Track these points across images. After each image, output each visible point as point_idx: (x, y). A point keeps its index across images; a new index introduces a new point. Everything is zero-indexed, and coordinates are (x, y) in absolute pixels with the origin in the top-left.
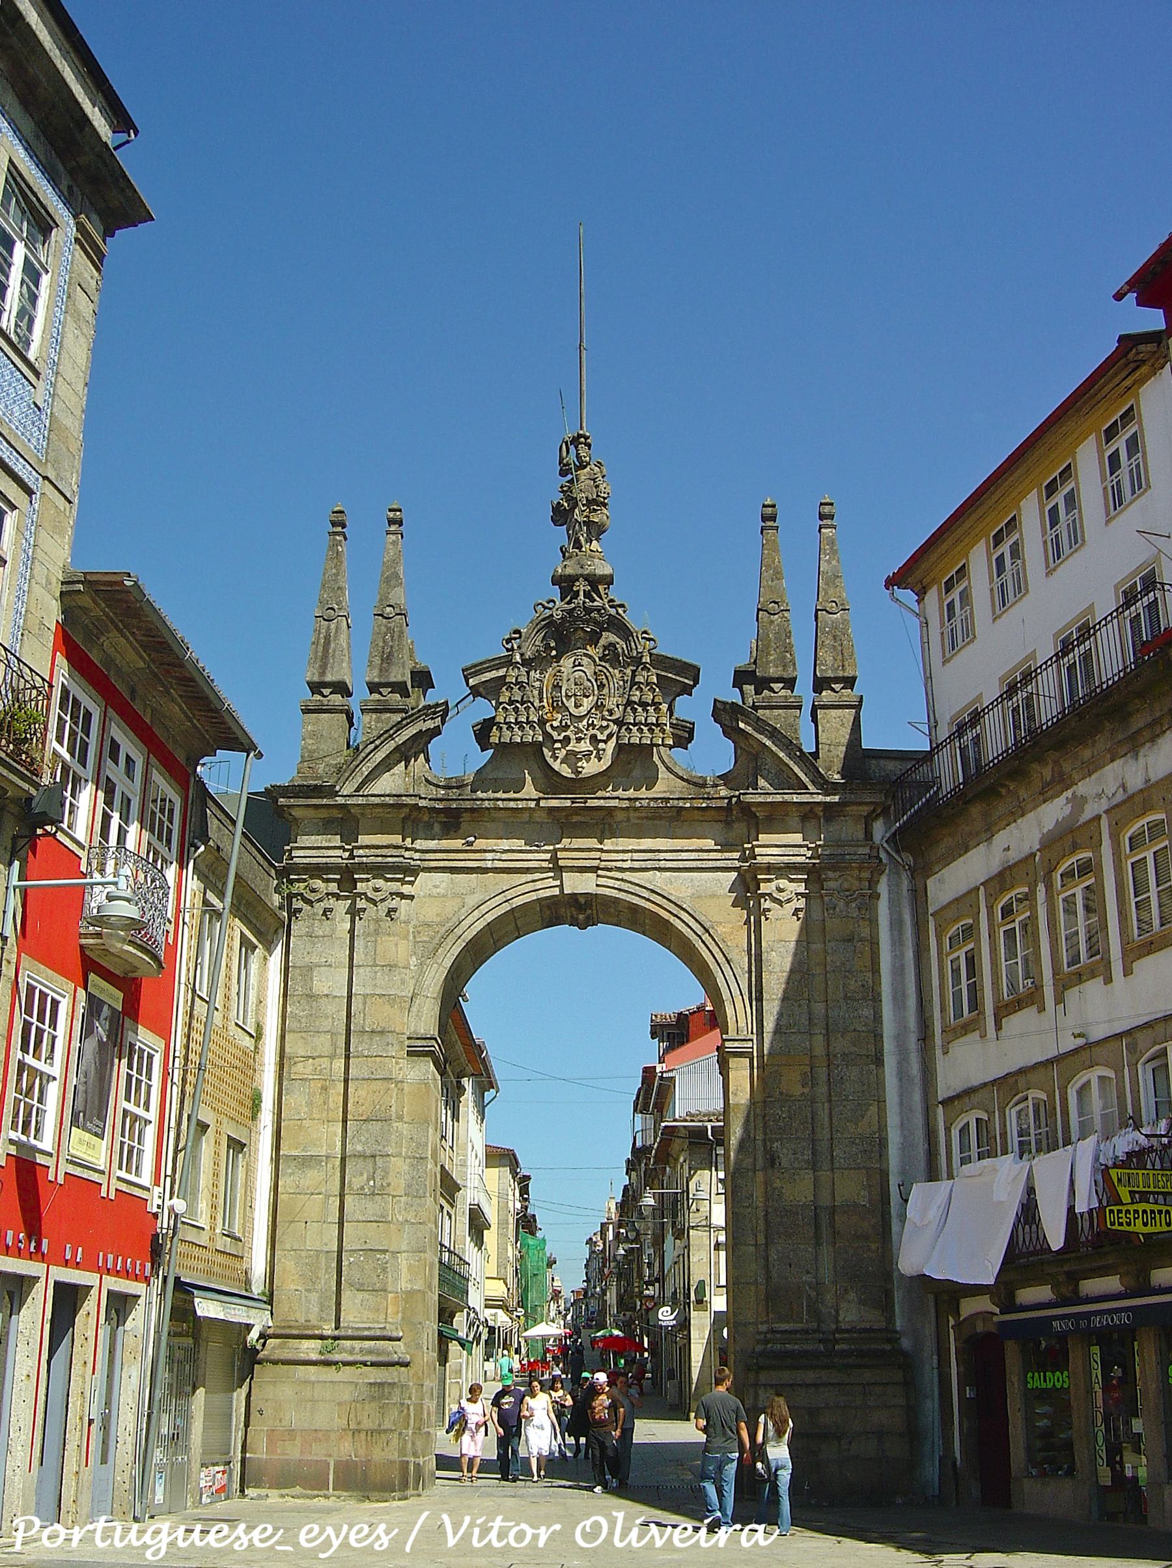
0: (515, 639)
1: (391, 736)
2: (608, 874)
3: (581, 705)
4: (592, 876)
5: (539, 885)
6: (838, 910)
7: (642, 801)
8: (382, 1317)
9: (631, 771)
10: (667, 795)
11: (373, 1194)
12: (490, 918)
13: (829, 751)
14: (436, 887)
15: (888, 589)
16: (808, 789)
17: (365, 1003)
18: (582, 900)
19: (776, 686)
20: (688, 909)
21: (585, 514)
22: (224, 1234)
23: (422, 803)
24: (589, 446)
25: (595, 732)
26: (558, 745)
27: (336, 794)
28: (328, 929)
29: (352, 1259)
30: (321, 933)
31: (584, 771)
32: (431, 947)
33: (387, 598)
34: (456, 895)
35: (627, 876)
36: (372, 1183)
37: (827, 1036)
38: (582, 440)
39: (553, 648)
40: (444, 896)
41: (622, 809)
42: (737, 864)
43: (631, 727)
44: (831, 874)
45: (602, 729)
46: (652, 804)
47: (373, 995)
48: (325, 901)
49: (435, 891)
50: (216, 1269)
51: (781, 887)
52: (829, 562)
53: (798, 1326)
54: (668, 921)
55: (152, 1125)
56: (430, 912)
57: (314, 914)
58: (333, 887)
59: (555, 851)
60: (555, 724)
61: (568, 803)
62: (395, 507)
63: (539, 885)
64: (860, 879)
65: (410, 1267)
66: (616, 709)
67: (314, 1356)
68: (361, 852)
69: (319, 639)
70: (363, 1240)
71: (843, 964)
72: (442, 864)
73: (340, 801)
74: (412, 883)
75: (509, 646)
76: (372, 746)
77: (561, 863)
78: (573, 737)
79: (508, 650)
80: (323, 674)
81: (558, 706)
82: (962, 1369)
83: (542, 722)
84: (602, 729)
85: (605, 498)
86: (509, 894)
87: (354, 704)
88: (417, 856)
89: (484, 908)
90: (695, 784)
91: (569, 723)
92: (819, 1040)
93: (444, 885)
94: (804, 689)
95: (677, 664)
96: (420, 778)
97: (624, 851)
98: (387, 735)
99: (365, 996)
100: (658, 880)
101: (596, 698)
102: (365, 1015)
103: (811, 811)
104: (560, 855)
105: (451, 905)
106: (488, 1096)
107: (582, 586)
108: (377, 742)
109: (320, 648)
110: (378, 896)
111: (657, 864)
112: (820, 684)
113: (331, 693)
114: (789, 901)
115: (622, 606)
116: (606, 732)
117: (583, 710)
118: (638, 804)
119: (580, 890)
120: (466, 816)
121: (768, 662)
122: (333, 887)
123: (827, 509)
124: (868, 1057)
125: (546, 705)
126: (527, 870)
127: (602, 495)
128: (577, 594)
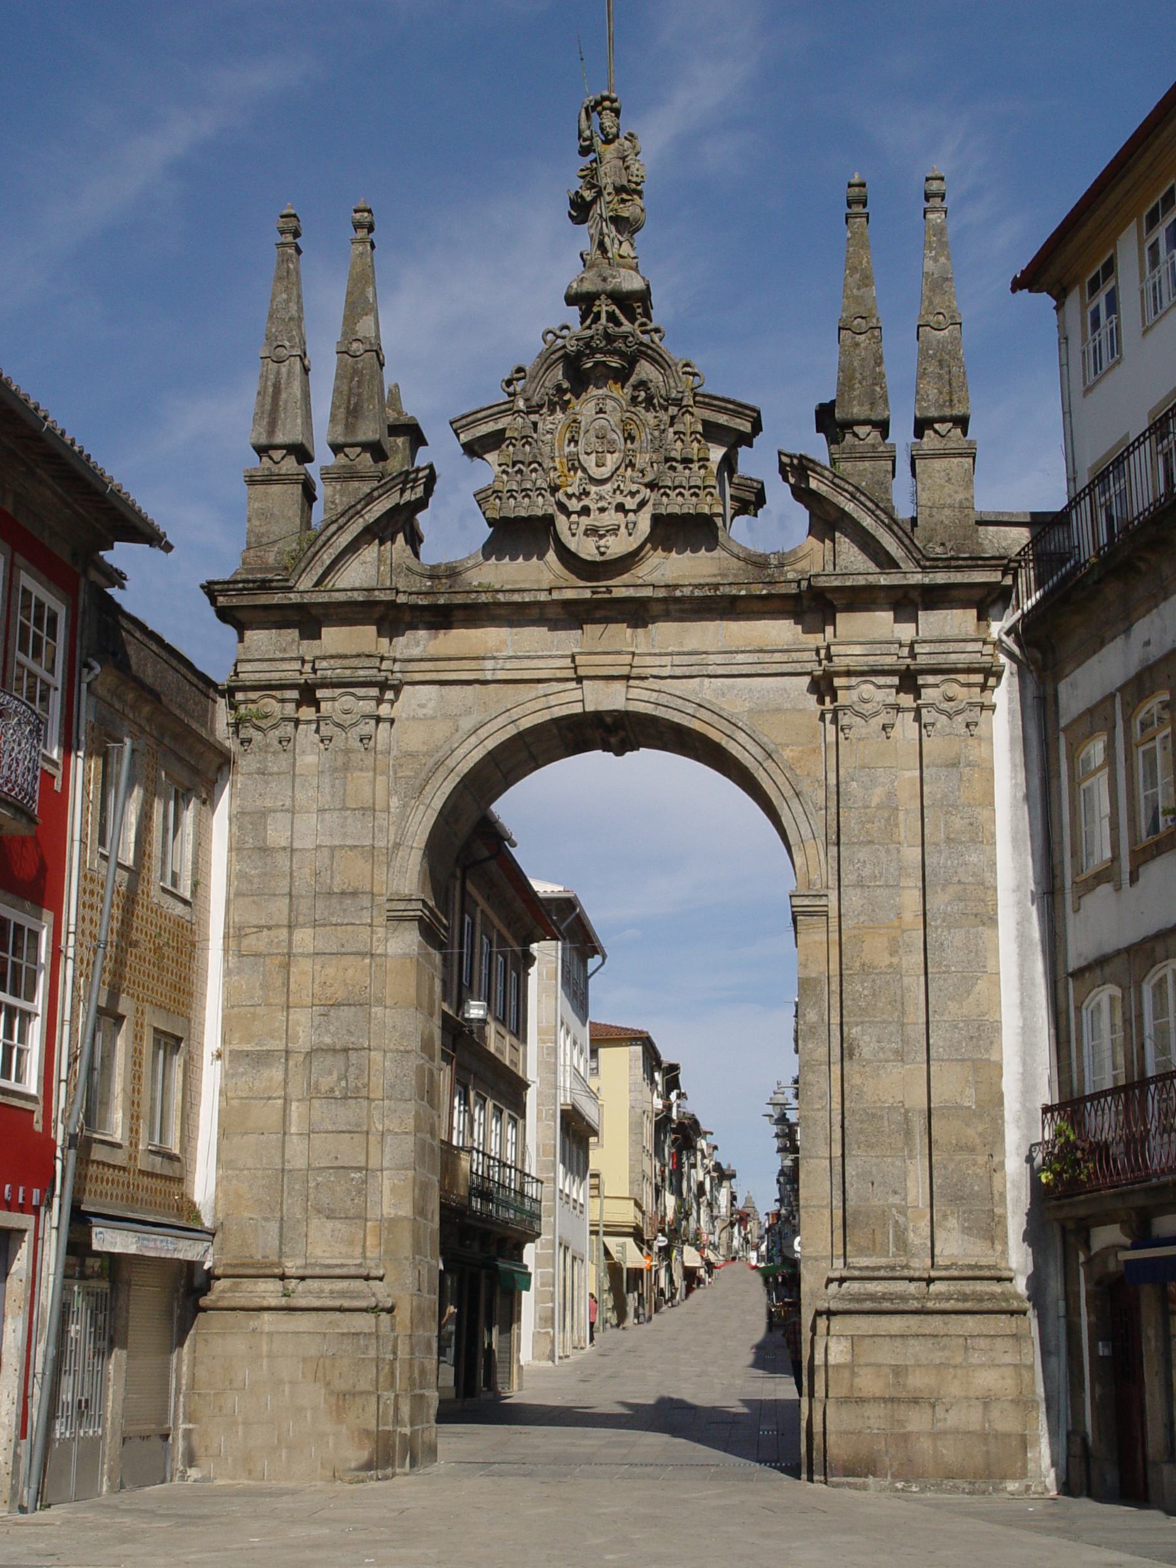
0: (518, 379)
1: (358, 513)
3: (603, 465)
4: (619, 686)
5: (553, 700)
7: (685, 589)
8: (358, 1250)
10: (718, 580)
11: (345, 1098)
12: (491, 744)
13: (931, 516)
14: (421, 706)
16: (900, 567)
18: (608, 720)
19: (862, 430)
20: (744, 728)
21: (611, 206)
22: (151, 1151)
23: (402, 599)
24: (617, 112)
25: (619, 498)
27: (290, 589)
28: (284, 764)
29: (320, 1179)
30: (275, 769)
31: (609, 552)
32: (418, 782)
33: (354, 332)
34: (446, 717)
36: (343, 1083)
38: (607, 104)
39: (565, 391)
40: (433, 718)
41: (658, 600)
43: (668, 491)
44: (930, 679)
45: (633, 494)
46: (697, 593)
47: (342, 847)
48: (280, 729)
49: (421, 712)
50: (141, 1194)
52: (935, 260)
53: (882, 1261)
55: (38, 1019)
57: (268, 745)
59: (573, 657)
60: (570, 490)
62: (362, 206)
63: (553, 700)
65: (393, 1190)
66: (649, 469)
67: (273, 1302)
68: (324, 664)
69: (265, 387)
70: (332, 1155)
71: (945, 796)
73: (294, 598)
75: (511, 389)
76: (334, 527)
77: (582, 672)
78: (593, 506)
79: (510, 395)
80: (271, 432)
81: (575, 465)
82: (1093, 1319)
84: (633, 494)
85: (638, 184)
86: (515, 713)
87: (313, 470)
89: (483, 733)
90: (754, 564)
93: (432, 704)
94: (901, 435)
96: (399, 565)
97: (660, 655)
98: (352, 512)
99: (333, 849)
100: (706, 689)
102: (332, 872)
103: (905, 596)
105: (441, 730)
106: (593, 963)
107: (604, 307)
108: (342, 521)
109: (269, 400)
110: (348, 719)
112: (921, 426)
114: (876, 714)
115: (657, 331)
116: (638, 498)
117: (604, 472)
118: (678, 593)
120: (459, 615)
121: (851, 400)
122: (290, 708)
123: (935, 186)
124: (976, 915)
125: (558, 467)
126: (539, 681)
127: (634, 179)
128: (597, 317)
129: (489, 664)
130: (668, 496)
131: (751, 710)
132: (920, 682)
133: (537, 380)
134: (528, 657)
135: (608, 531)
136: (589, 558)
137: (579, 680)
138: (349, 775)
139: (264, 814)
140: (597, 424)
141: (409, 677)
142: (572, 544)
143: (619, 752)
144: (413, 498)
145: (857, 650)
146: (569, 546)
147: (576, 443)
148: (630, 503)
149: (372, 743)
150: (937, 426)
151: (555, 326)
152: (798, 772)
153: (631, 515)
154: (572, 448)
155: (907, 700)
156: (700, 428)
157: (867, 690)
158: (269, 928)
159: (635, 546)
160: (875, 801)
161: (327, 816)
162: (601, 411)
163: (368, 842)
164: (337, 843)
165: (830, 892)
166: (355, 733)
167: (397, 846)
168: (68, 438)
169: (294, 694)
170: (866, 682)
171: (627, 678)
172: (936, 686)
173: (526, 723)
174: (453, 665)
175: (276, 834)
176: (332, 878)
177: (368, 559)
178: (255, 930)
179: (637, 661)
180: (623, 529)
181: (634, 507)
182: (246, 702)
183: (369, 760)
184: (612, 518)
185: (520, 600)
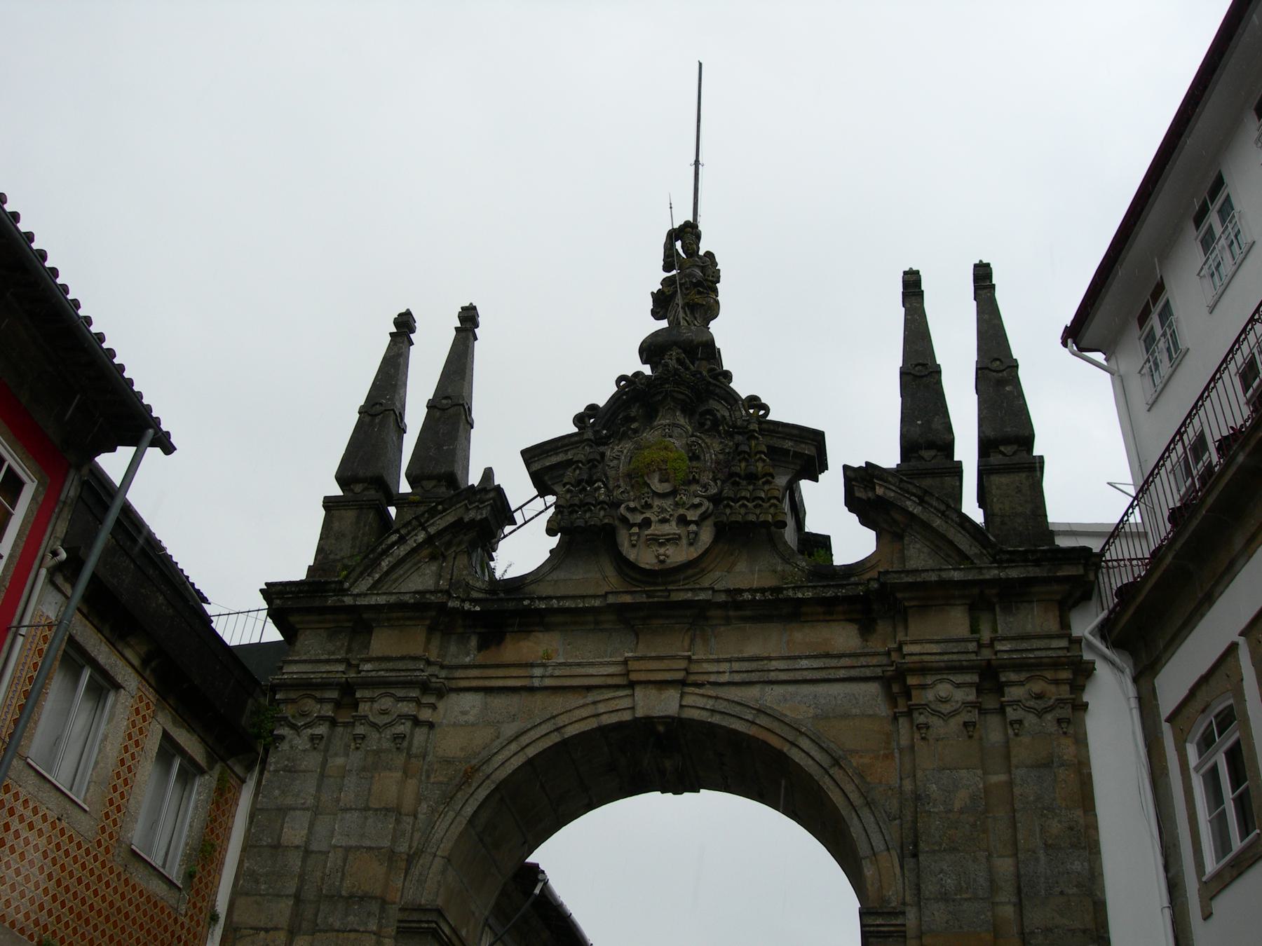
2: (697, 691)
5: (602, 708)
6: (1026, 724)
9: (734, 564)
12: (531, 752)
15: (1065, 344)
17: (345, 860)
20: (809, 733)
25: (681, 511)
26: (635, 530)
27: (344, 592)
31: (668, 561)
35: (721, 692)
37: (1019, 906)
40: (473, 725)
42: (879, 671)
44: (1013, 677)
47: (358, 848)
49: (462, 719)
51: (943, 694)
54: (780, 753)
56: (451, 744)
58: (328, 710)
59: (625, 662)
60: (632, 505)
61: (644, 599)
63: (602, 708)
64: (1056, 682)
66: (712, 483)
68: (368, 667)
72: (474, 683)
73: (348, 600)
74: (434, 707)
77: (634, 677)
78: (654, 518)
83: (617, 505)
86: (561, 721)
88: (443, 674)
89: (525, 740)
91: (650, 501)
92: (1008, 911)
95: (795, 432)
97: (718, 661)
99: (348, 849)
102: (343, 874)
104: (633, 665)
111: (765, 677)
113: (364, 490)
119: (657, 712)
122: (328, 710)
124: (1084, 931)
125: (622, 485)
126: (589, 688)
127: (711, 278)
129: (538, 672)
130: (731, 507)
131: (816, 717)
132: (1003, 679)
134: (579, 664)
135: (668, 540)
136: (648, 567)
137: (632, 685)
138: (377, 775)
139: (283, 811)
141: (453, 684)
142: (632, 555)
143: (677, 791)
144: (479, 517)
145: (934, 648)
148: (692, 515)
149: (405, 744)
150: (1002, 448)
152: (869, 779)
153: (693, 528)
155: (990, 702)
157: (944, 689)
158: (267, 930)
159: (695, 555)
160: (957, 805)
161: (348, 816)
163: (386, 843)
164: (353, 842)
165: (908, 909)
166: (388, 733)
167: (419, 853)
168: (23, 226)
169: (334, 694)
170: (941, 681)
171: (683, 683)
172: (1021, 683)
173: (571, 731)
174: (500, 672)
175: (294, 832)
176: (342, 880)
177: (428, 571)
178: (252, 932)
179: (694, 668)
180: (684, 541)
182: (286, 701)
183: (400, 760)
184: (672, 528)
185: (573, 606)
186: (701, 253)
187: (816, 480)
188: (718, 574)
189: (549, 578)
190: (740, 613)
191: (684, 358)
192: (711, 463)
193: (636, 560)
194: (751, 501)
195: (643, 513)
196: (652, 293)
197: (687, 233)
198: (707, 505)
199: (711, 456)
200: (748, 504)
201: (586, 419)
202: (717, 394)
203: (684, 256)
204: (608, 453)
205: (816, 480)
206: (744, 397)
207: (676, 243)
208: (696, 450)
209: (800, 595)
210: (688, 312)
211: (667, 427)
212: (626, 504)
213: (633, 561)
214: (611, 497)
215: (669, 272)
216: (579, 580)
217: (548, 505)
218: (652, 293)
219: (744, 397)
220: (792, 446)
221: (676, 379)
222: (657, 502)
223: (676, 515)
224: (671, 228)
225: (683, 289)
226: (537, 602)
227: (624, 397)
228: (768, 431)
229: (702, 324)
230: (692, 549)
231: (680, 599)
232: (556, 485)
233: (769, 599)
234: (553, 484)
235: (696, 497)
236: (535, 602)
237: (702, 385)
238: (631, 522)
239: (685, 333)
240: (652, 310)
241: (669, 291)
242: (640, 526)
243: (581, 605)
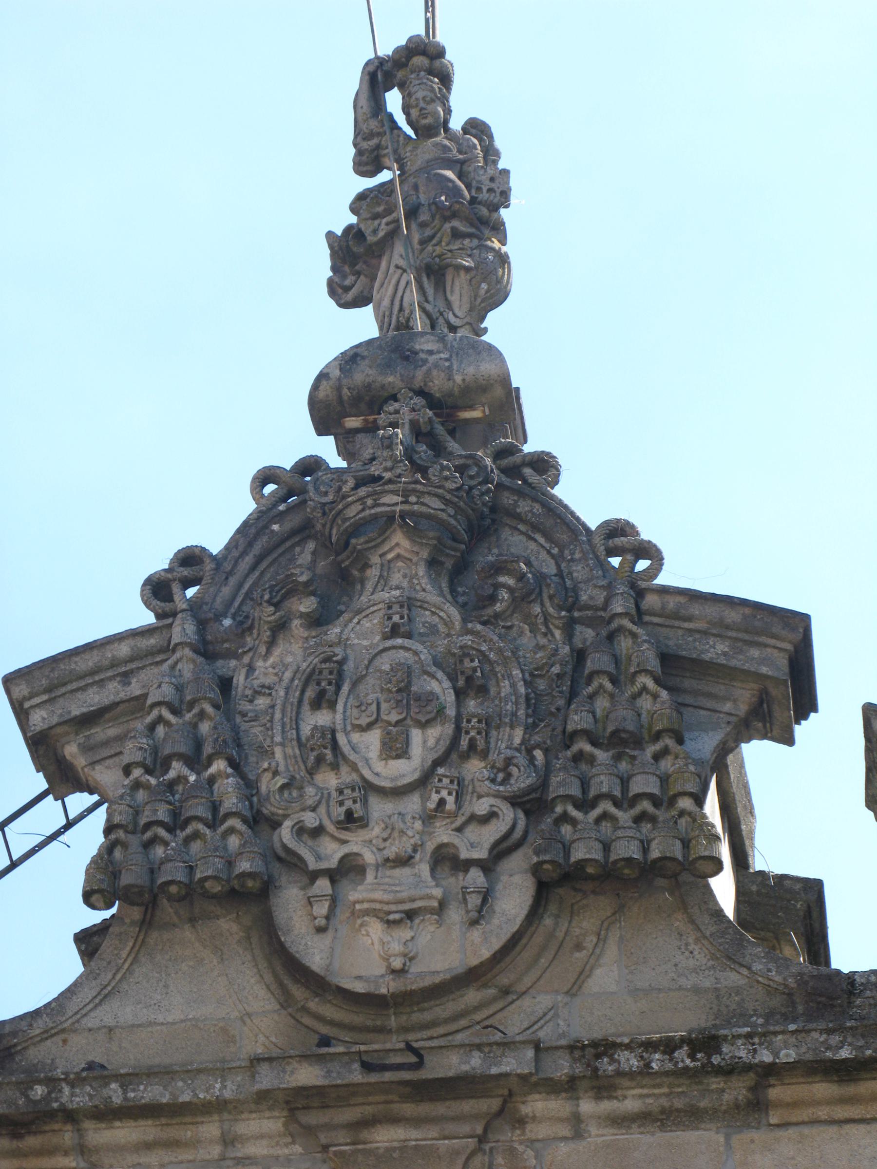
9: (583, 975)
25: (443, 834)
26: (323, 885)
31: (415, 969)
60: (310, 820)
66: (521, 759)
78: (369, 857)
95: (733, 616)
101: (449, 729)
130: (574, 822)
133: (233, 581)
140: (385, 663)
146: (307, 961)
147: (332, 705)
151: (288, 464)
153: (476, 877)
154: (323, 718)
156: (654, 664)
159: (486, 953)
162: (395, 631)
181: (481, 854)
186: (456, 124)
187: (789, 740)
188: (544, 1001)
189: (90, 1022)
190: (607, 1106)
191: (429, 418)
192: (517, 703)
193: (328, 967)
194: (625, 805)
195: (344, 842)
196: (330, 235)
197: (417, 70)
198: (508, 814)
199: (513, 685)
200: (618, 813)
201: (176, 588)
202: (519, 518)
203: (410, 132)
204: (240, 680)
205: (789, 740)
206: (593, 524)
207: (387, 94)
208: (474, 670)
209: (766, 1057)
210: (430, 291)
211: (396, 608)
212: (295, 818)
213: (322, 974)
214: (255, 799)
215: (372, 174)
216: (173, 1024)
217: (71, 817)
218: (330, 235)
219: (593, 526)
220: (725, 654)
221: (417, 482)
222: (379, 808)
223: (430, 846)
224: (372, 56)
225: (414, 226)
226: (67, 1090)
227: (276, 527)
228: (660, 616)
229: (467, 320)
230: (476, 934)
231: (451, 1074)
232: (98, 767)
233: (686, 1068)
234: (93, 764)
235: (480, 797)
236: (60, 1091)
237: (483, 494)
238: (312, 865)
239: (431, 352)
240: (330, 283)
241: (375, 232)
242: (334, 875)
243: (186, 1097)
